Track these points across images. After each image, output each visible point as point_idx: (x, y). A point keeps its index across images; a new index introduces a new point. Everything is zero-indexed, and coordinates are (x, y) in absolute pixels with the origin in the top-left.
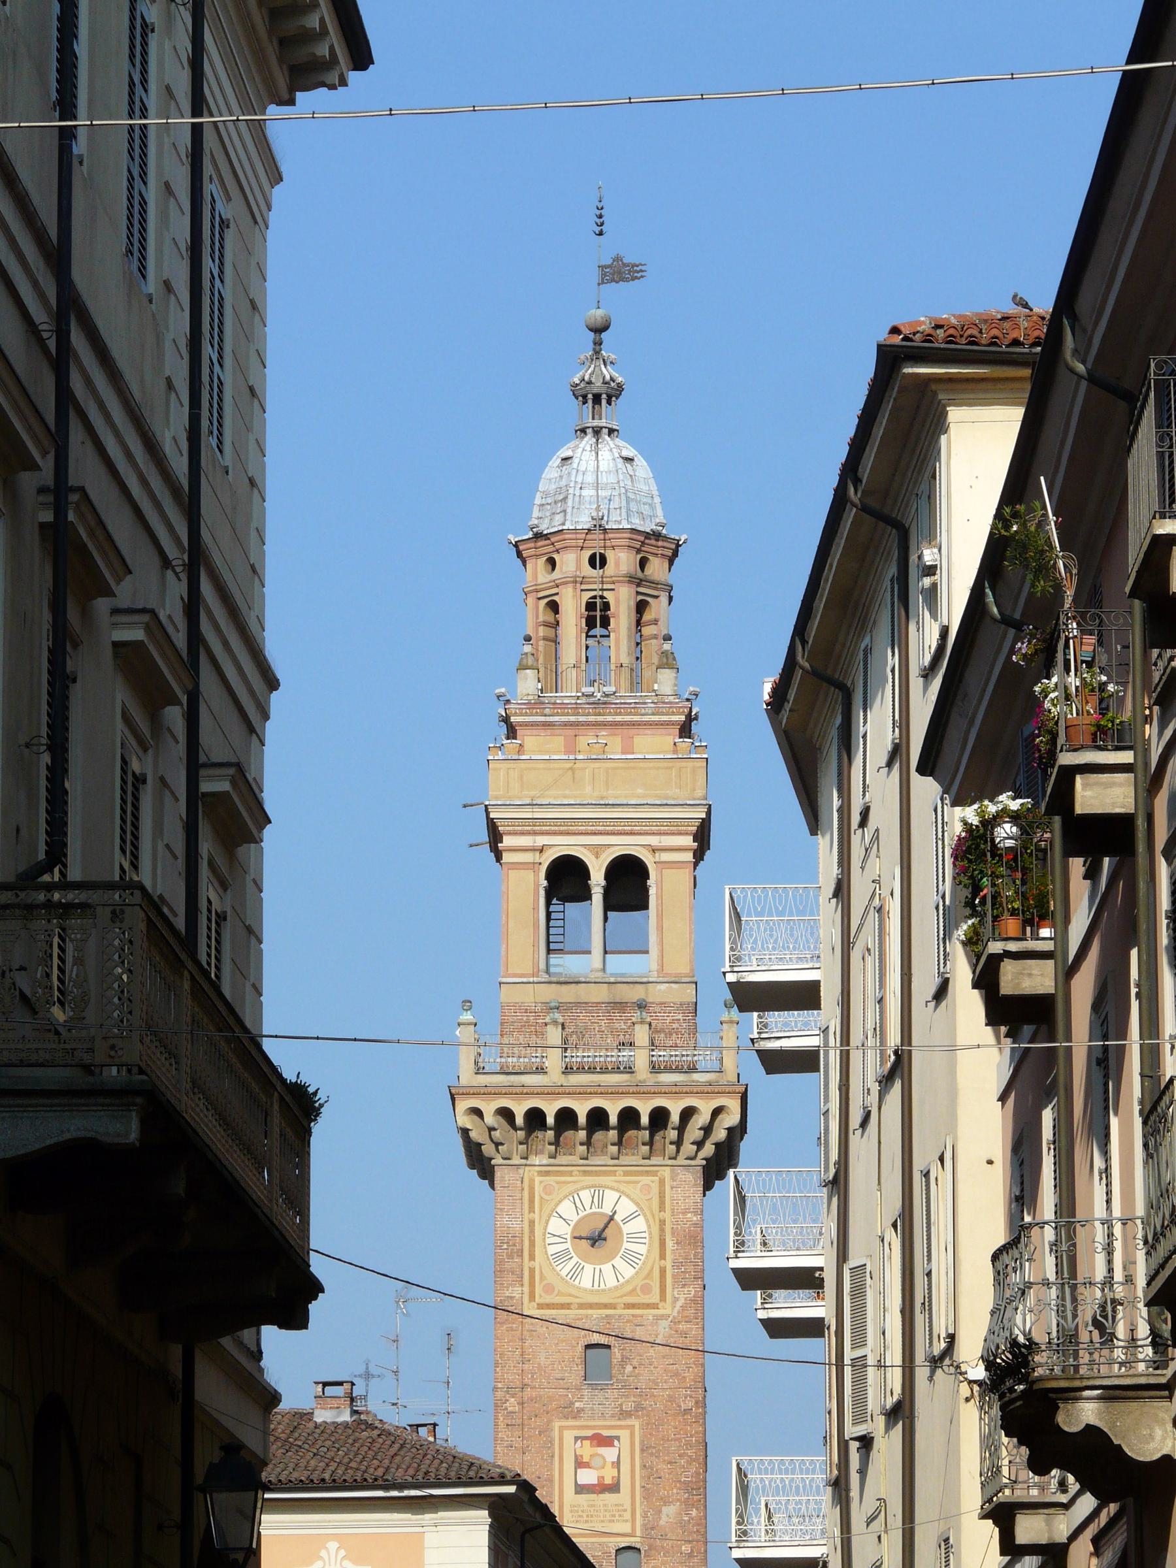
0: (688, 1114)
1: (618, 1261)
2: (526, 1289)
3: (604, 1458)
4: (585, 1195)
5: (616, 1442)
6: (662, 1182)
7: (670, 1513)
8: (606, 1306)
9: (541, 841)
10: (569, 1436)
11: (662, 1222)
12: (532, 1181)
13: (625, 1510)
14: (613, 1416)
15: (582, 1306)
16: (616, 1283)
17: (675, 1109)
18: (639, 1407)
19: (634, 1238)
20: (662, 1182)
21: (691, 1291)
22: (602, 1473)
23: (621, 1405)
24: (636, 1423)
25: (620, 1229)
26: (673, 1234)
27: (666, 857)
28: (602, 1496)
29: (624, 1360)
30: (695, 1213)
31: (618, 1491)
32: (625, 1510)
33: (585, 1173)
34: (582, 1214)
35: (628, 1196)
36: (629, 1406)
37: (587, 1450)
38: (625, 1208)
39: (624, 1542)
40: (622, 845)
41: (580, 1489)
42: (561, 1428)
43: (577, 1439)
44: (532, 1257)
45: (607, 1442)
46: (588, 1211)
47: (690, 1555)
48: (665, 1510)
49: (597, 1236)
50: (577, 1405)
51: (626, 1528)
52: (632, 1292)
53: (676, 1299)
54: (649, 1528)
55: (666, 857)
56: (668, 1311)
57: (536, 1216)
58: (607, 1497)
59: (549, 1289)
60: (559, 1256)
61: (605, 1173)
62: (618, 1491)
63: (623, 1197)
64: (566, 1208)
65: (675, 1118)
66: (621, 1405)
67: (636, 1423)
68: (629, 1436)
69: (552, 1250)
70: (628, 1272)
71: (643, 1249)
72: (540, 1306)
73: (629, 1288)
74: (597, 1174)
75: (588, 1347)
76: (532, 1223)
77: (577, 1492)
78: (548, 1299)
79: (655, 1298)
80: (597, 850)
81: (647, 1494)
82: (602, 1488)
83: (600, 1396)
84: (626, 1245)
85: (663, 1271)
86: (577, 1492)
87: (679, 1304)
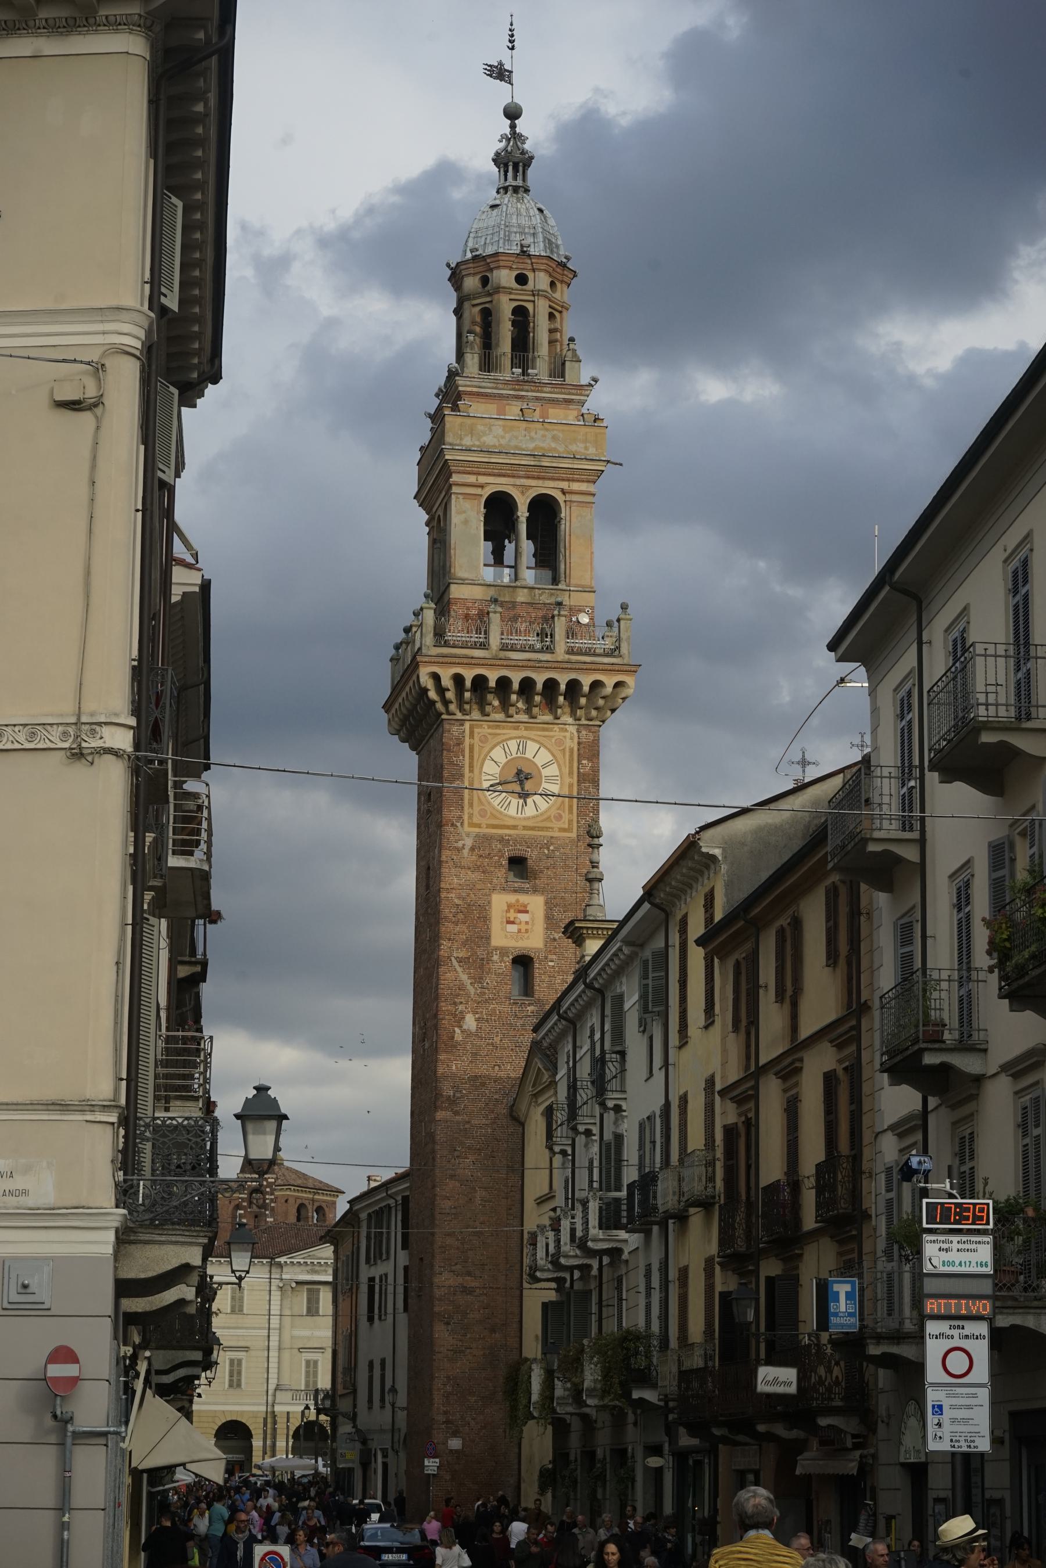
0: (596, 685)
4: (513, 745)
9: (482, 479)
17: (586, 681)
19: (549, 779)
27: (575, 498)
34: (509, 758)
35: (546, 748)
38: (543, 757)
46: (514, 755)
49: (521, 780)
52: (548, 819)
73: (545, 817)
80: (524, 489)
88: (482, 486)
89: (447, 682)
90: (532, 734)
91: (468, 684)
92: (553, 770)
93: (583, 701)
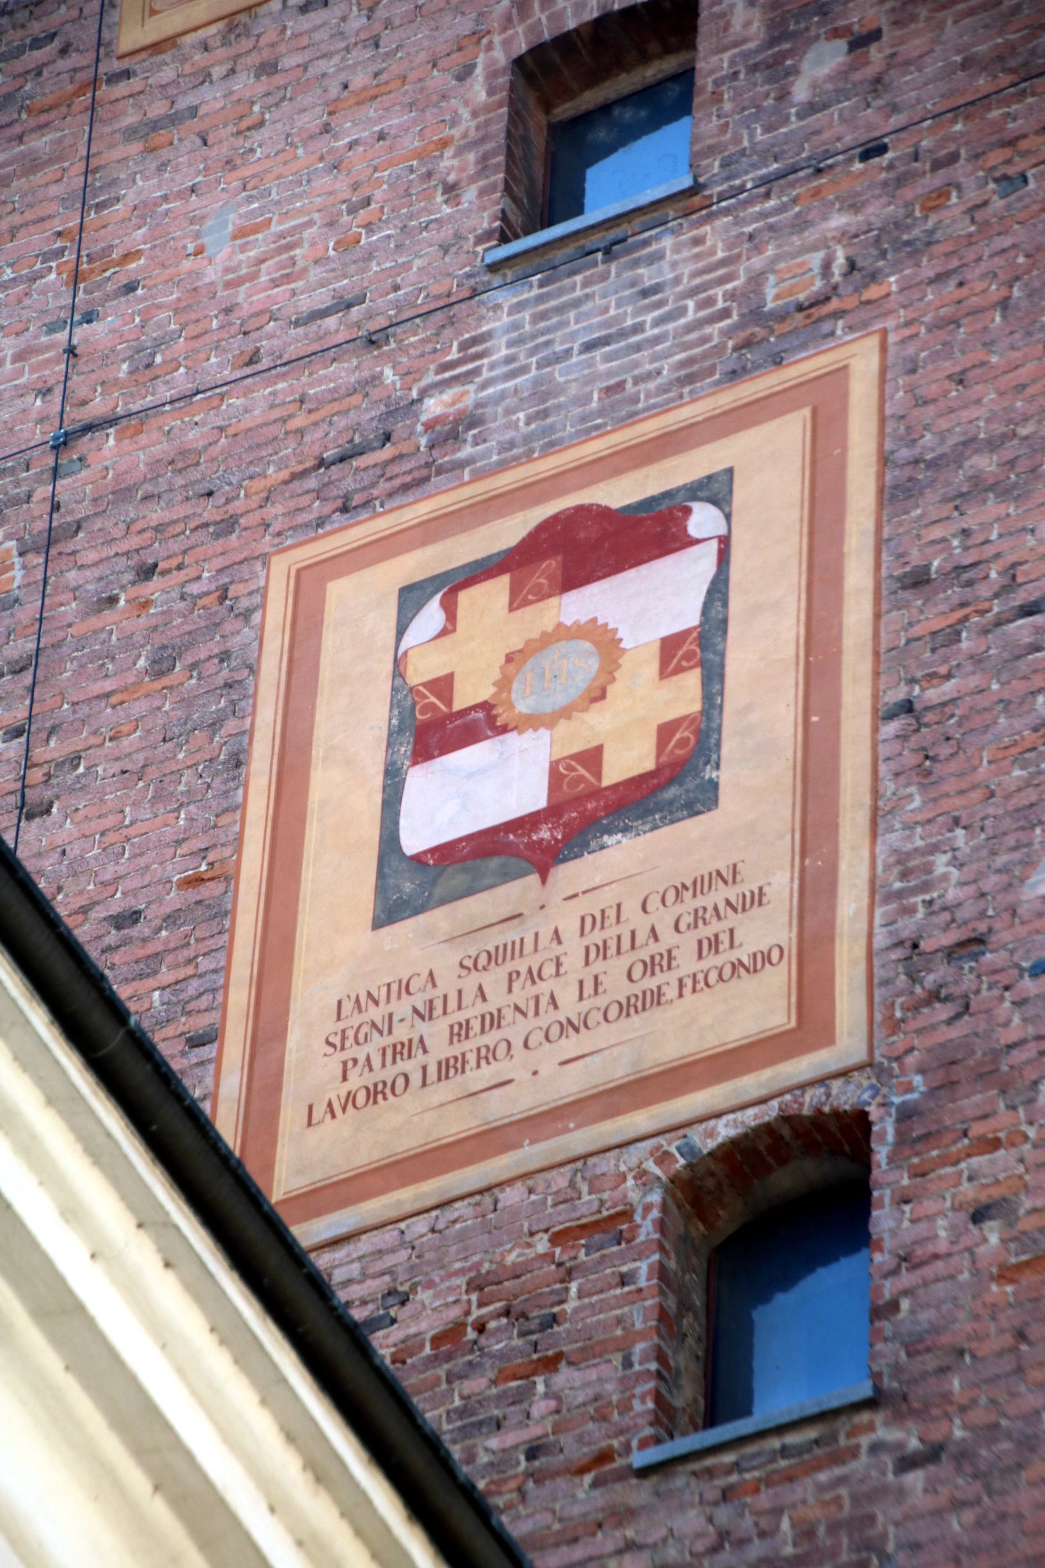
3: (606, 642)
5: (703, 520)
10: (359, 608)
13: (759, 898)
14: (689, 377)
22: (595, 725)
23: (757, 280)
24: (861, 359)
28: (569, 875)
31: (706, 798)
32: (759, 898)
36: (791, 271)
37: (477, 645)
39: (724, 1112)
41: (412, 882)
43: (411, 599)
45: (648, 533)
50: (434, 406)
51: (761, 1006)
54: (934, 963)
58: (624, 863)
66: (757, 280)
67: (861, 359)
77: (390, 911)
83: (600, 296)
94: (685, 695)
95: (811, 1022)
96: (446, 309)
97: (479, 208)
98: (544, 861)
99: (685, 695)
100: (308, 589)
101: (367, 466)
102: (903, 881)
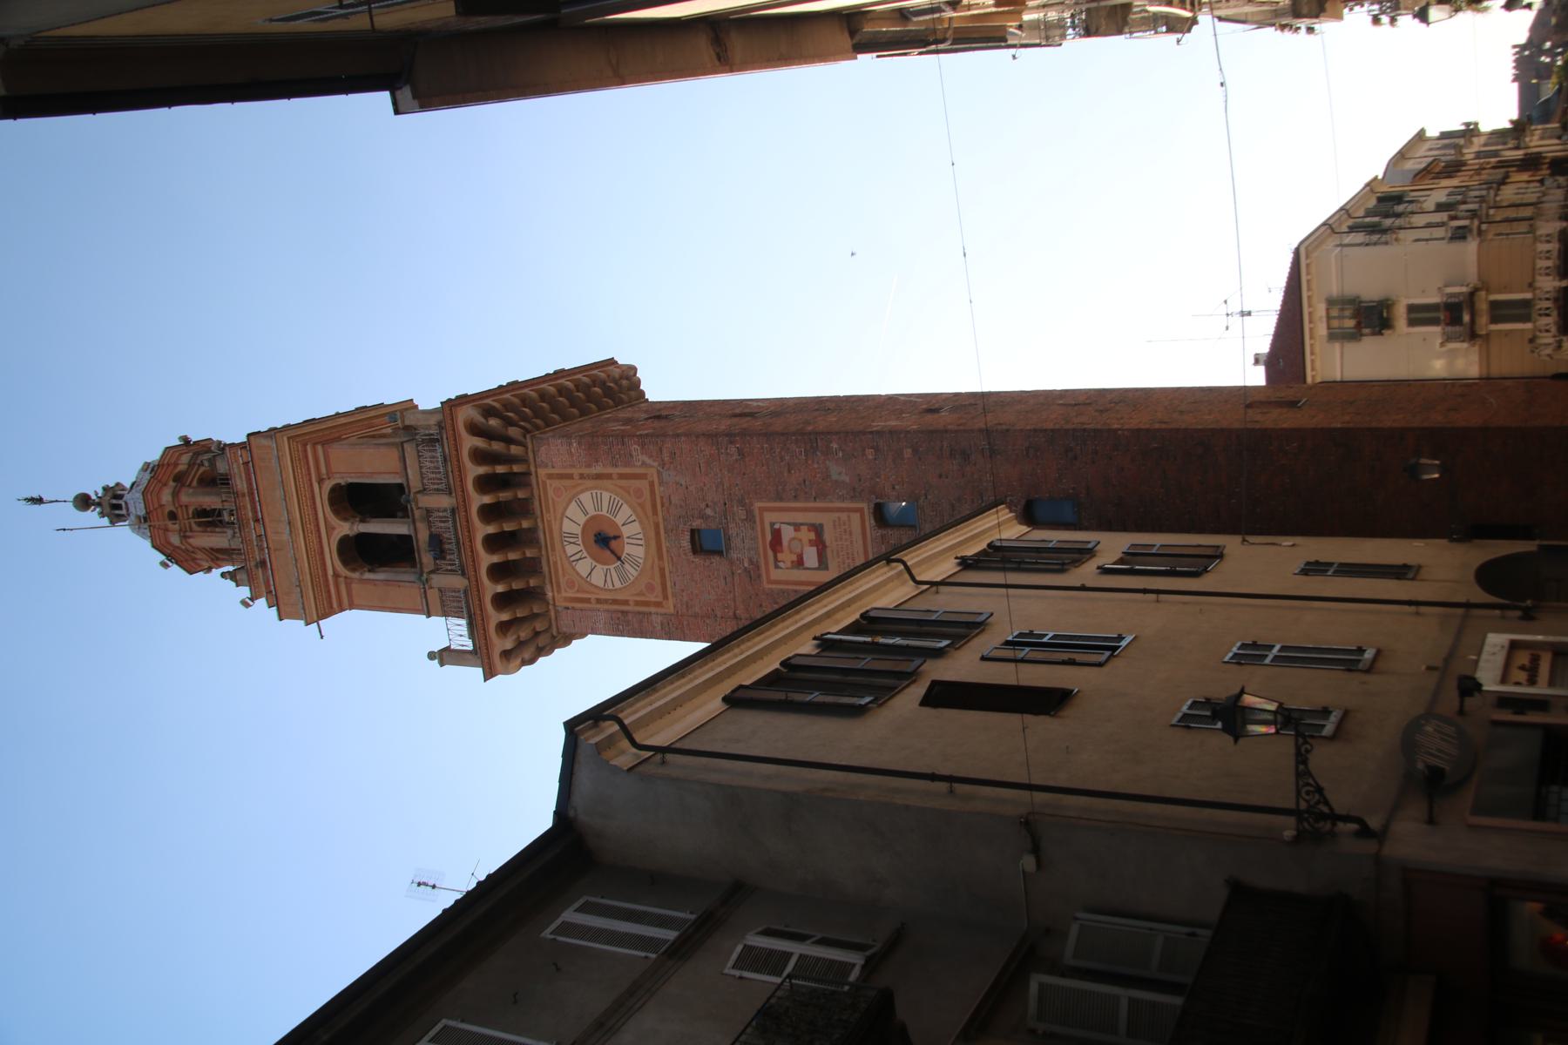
0: (479, 456)
1: (619, 520)
2: (653, 610)
4: (571, 549)
6: (550, 476)
7: (838, 472)
8: (658, 534)
10: (776, 574)
11: (582, 476)
12: (566, 599)
15: (661, 557)
16: (636, 524)
18: (741, 502)
19: (598, 503)
20: (550, 476)
21: (635, 448)
22: (805, 541)
24: (758, 505)
25: (593, 518)
26: (589, 466)
27: (323, 470)
29: (703, 516)
30: (570, 444)
31: (821, 526)
33: (553, 550)
36: (742, 514)
37: (787, 557)
39: (870, 521)
40: (323, 509)
41: (823, 564)
42: (770, 582)
43: (777, 567)
44: (626, 602)
45: (777, 534)
47: (877, 449)
48: (835, 477)
49: (604, 541)
51: (856, 517)
53: (644, 463)
54: (854, 494)
55: (323, 470)
56: (653, 471)
57: (593, 597)
58: (828, 537)
59: (650, 588)
60: (622, 578)
61: (551, 531)
62: (821, 526)
63: (568, 513)
64: (583, 567)
65: (482, 470)
68: (773, 516)
69: (618, 585)
70: (625, 512)
71: (606, 496)
72: (666, 597)
73: (639, 510)
74: (552, 538)
75: (695, 551)
76: (599, 601)
77: (827, 568)
78: (659, 589)
79: (643, 485)
81: (821, 495)
82: (820, 544)
84: (604, 512)
85: (622, 476)
86: (827, 568)
87: (648, 461)
88: (336, 575)
89: (509, 644)
90: (555, 528)
91: (505, 617)
92: (586, 498)
93: (500, 469)
94: (804, 528)
95: (861, 511)
96: (732, 563)
97: (716, 559)
98: (825, 546)
99: (804, 528)
100: (770, 582)
101: (753, 573)
102: (842, 498)
